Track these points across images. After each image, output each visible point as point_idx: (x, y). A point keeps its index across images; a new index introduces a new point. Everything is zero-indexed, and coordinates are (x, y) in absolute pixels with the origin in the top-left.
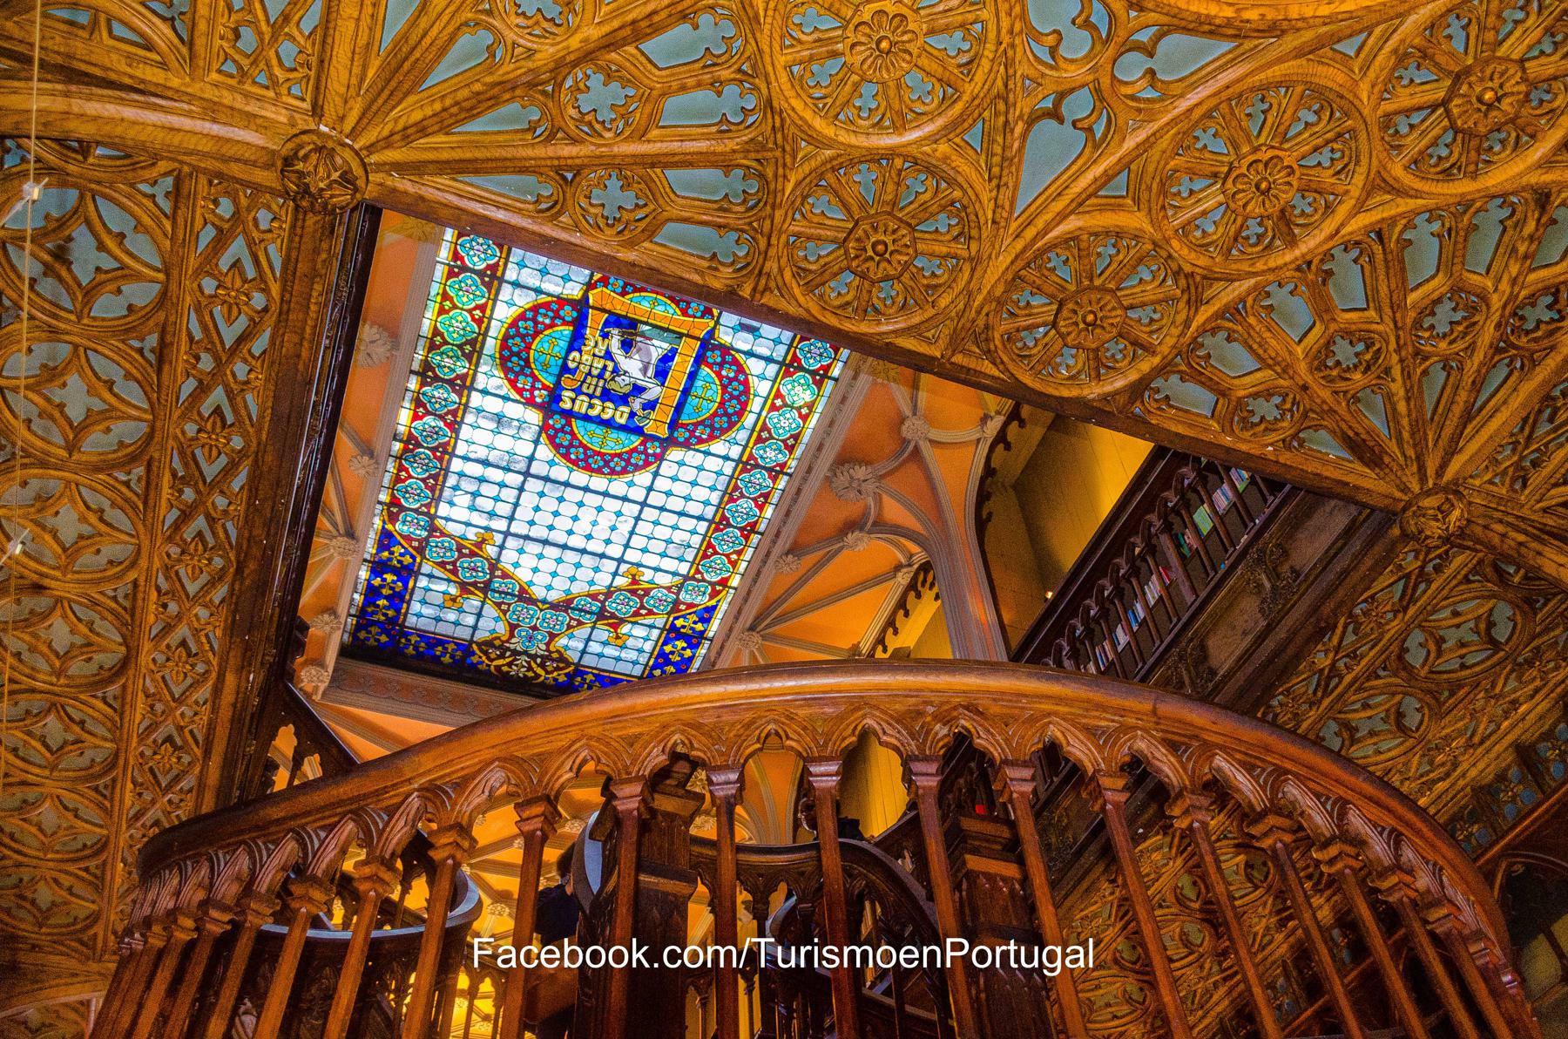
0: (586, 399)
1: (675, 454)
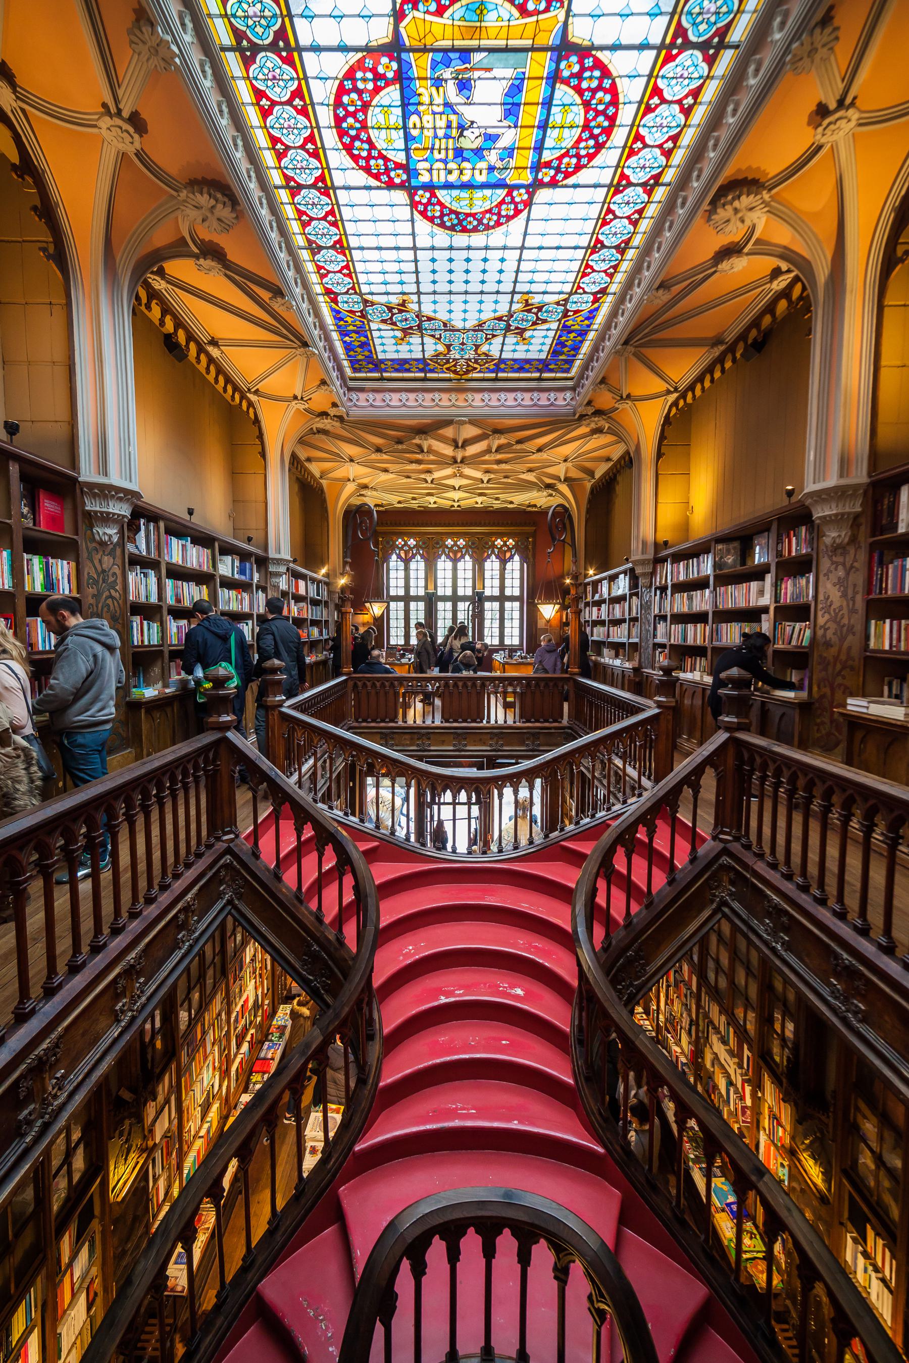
0: (440, 165)
1: (543, 195)
